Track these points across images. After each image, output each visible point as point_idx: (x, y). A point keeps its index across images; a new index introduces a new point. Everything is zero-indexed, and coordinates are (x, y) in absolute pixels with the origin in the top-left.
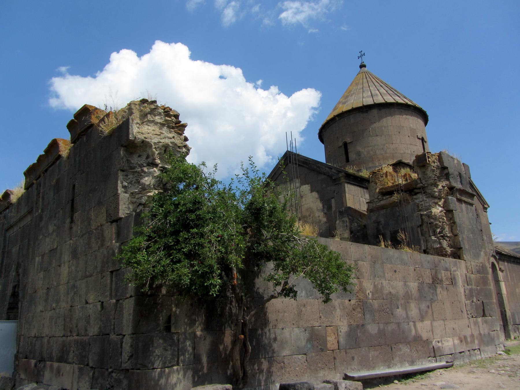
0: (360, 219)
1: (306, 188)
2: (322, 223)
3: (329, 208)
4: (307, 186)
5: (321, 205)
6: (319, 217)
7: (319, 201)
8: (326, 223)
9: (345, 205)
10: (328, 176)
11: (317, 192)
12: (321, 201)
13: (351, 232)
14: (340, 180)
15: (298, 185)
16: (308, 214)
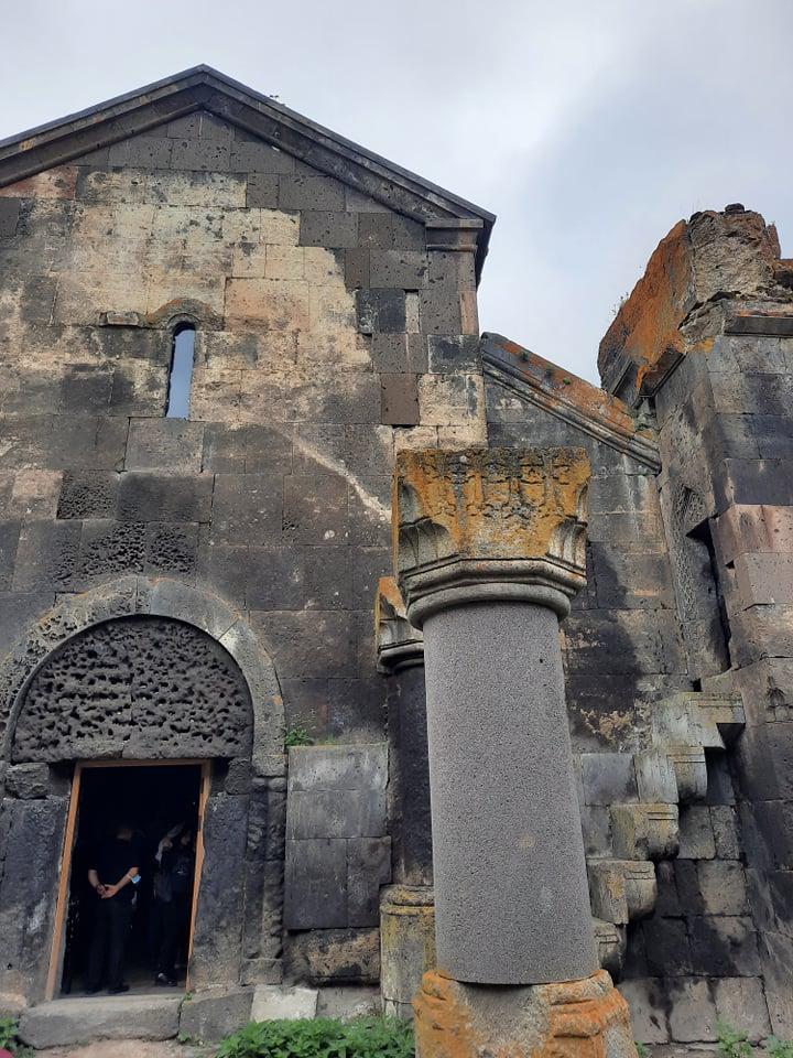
0: (546, 388)
1: (278, 226)
2: (348, 363)
3: (393, 321)
4: (279, 214)
5: (348, 302)
6: (332, 339)
7: (339, 282)
8: (369, 369)
9: (467, 327)
10: (399, 213)
11: (337, 251)
12: (349, 287)
13: (493, 428)
14: (453, 241)
15: (238, 199)
16: (271, 316)
